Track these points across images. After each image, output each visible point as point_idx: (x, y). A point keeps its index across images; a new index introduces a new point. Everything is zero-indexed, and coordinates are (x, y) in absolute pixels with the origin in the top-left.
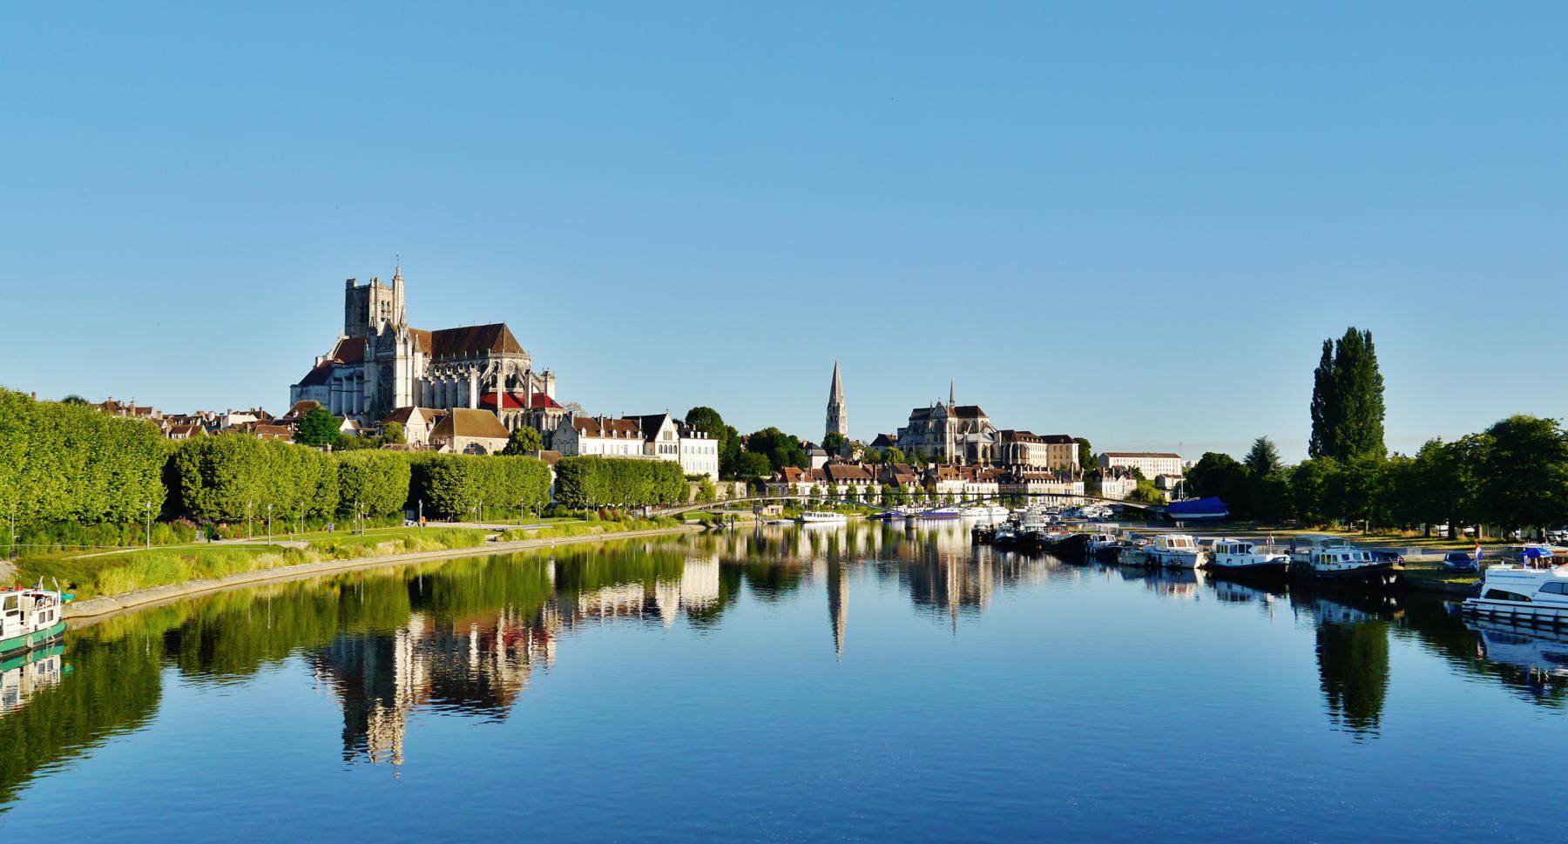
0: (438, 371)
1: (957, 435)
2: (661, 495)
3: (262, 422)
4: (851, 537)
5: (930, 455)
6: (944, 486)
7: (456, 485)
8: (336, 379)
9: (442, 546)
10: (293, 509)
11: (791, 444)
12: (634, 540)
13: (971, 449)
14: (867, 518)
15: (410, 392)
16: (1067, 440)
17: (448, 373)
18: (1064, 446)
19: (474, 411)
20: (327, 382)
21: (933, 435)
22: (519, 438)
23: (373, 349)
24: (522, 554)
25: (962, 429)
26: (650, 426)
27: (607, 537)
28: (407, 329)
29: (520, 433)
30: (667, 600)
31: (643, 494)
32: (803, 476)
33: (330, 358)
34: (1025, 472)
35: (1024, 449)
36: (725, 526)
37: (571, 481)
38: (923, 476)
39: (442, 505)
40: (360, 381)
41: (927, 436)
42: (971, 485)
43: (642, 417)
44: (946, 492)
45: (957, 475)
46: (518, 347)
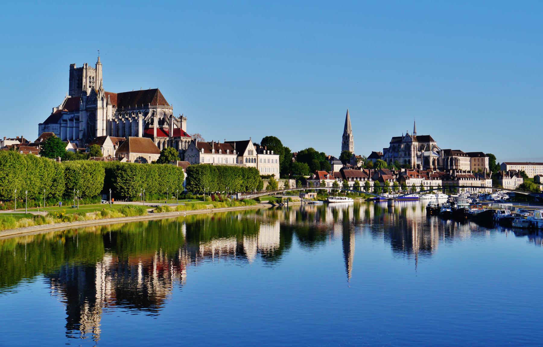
0: (120, 116)
2: (247, 187)
3: (22, 145)
4: (356, 211)
5: (402, 164)
6: (410, 182)
7: (130, 180)
8: (64, 120)
9: (122, 215)
10: (39, 193)
11: (321, 157)
12: (231, 213)
13: (426, 160)
14: (365, 200)
15: (105, 128)
16: (482, 155)
17: (126, 117)
18: (480, 158)
19: (141, 139)
20: (59, 122)
21: (404, 152)
22: (166, 154)
23: (84, 103)
24: (167, 220)
25: (421, 149)
27: (216, 210)
28: (103, 92)
29: (167, 151)
30: (250, 247)
31: (236, 186)
32: (328, 176)
33: (61, 108)
34: (457, 174)
35: (457, 160)
36: (283, 205)
37: (195, 179)
38: (398, 176)
39: (123, 192)
40: (77, 122)
41: (400, 153)
42: (426, 181)
43: (236, 142)
44: (411, 185)
45: (418, 176)
46: (166, 102)
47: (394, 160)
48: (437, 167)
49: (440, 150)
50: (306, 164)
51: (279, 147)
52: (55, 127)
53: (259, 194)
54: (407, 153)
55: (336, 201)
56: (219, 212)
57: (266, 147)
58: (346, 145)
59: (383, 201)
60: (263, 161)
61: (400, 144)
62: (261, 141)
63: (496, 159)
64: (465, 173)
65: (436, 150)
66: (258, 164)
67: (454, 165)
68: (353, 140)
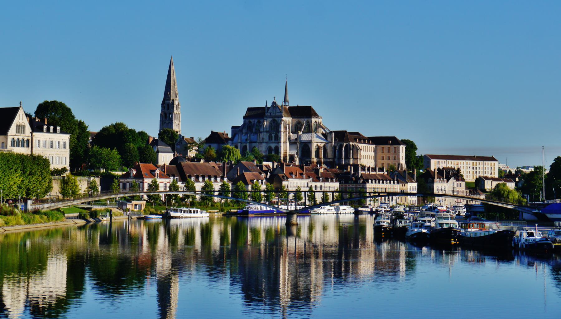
1: (291, 134)
2: (28, 189)
4: (206, 231)
5: (264, 154)
11: (140, 139)
13: (305, 148)
14: (223, 215)
16: (394, 141)
18: (392, 148)
21: (268, 134)
25: (296, 129)
27: (9, 229)
31: (10, 188)
34: (363, 172)
38: (269, 174)
41: (261, 135)
42: (314, 184)
44: (294, 189)
45: (301, 174)
47: (250, 147)
48: (322, 160)
49: (328, 132)
50: (115, 152)
51: (69, 121)
53: (67, 202)
54: (273, 135)
55: (182, 216)
56: (12, 233)
57: (46, 120)
58: (168, 118)
59: (254, 217)
60: (41, 144)
61: (261, 120)
62: (35, 109)
63: (416, 149)
64: (376, 171)
65: (321, 131)
66: (34, 149)
67: (351, 157)
68: (179, 110)
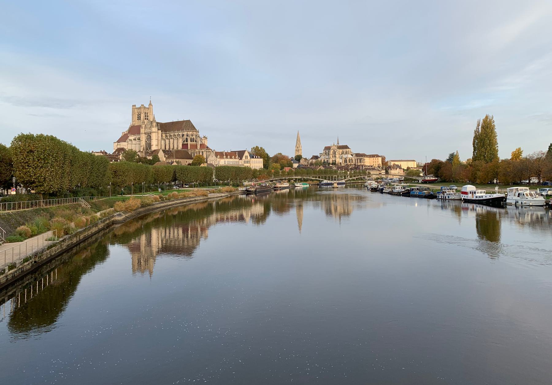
18: (377, 158)
20: (127, 141)
23: (144, 129)
26: (241, 154)
43: (238, 151)
46: (195, 128)
52: (124, 144)
